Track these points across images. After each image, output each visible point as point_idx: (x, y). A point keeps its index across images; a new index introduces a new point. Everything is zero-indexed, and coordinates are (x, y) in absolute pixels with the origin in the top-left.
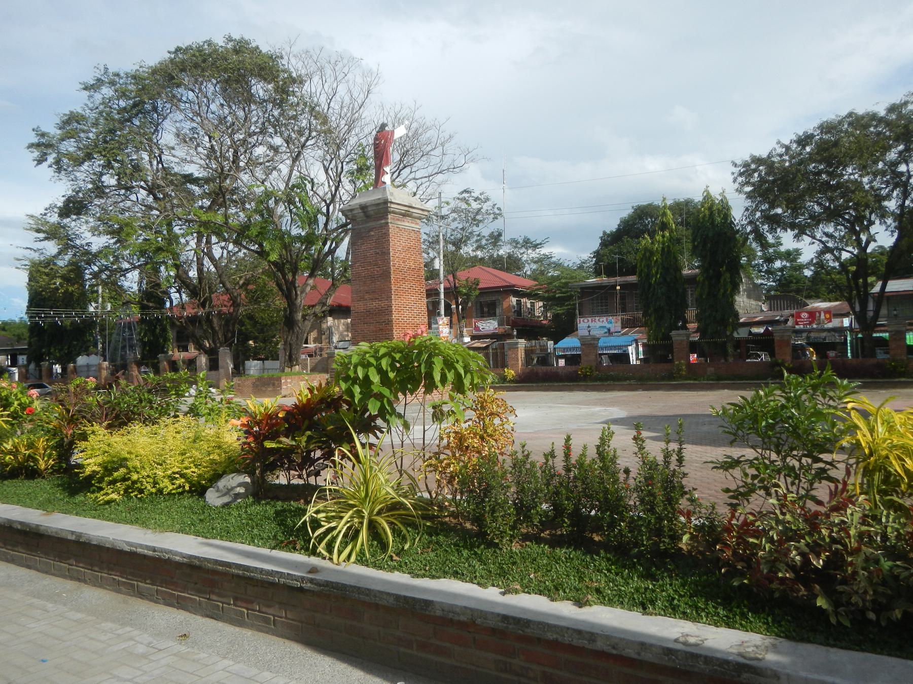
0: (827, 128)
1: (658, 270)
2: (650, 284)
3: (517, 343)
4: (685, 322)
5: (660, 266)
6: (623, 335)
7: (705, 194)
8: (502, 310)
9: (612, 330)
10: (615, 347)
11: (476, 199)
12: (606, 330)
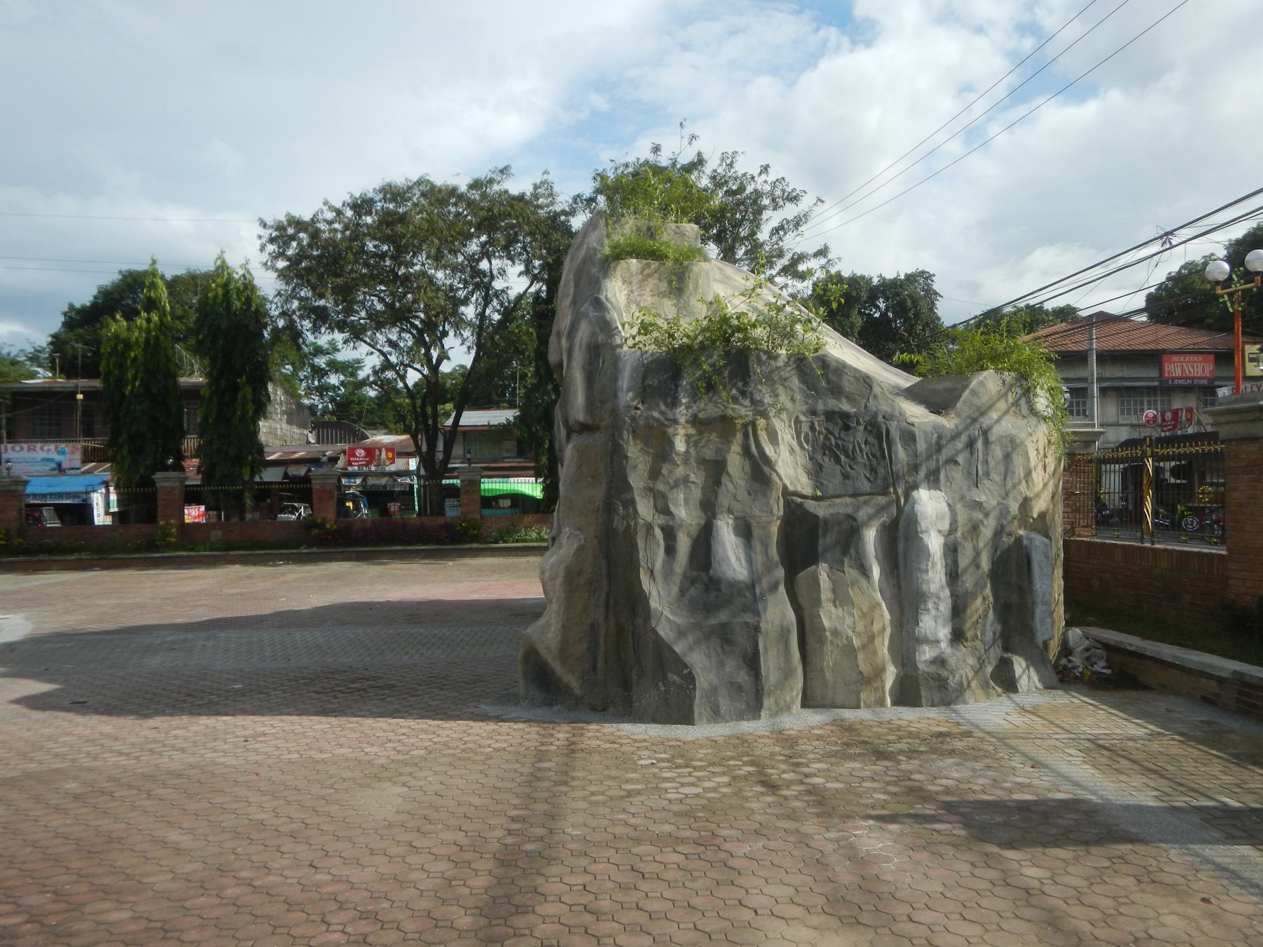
0: (392, 193)
1: (137, 371)
2: (124, 395)
4: (180, 457)
5: (141, 368)
6: (84, 473)
7: (219, 263)
9: (65, 465)
10: (68, 495)
12: (54, 466)
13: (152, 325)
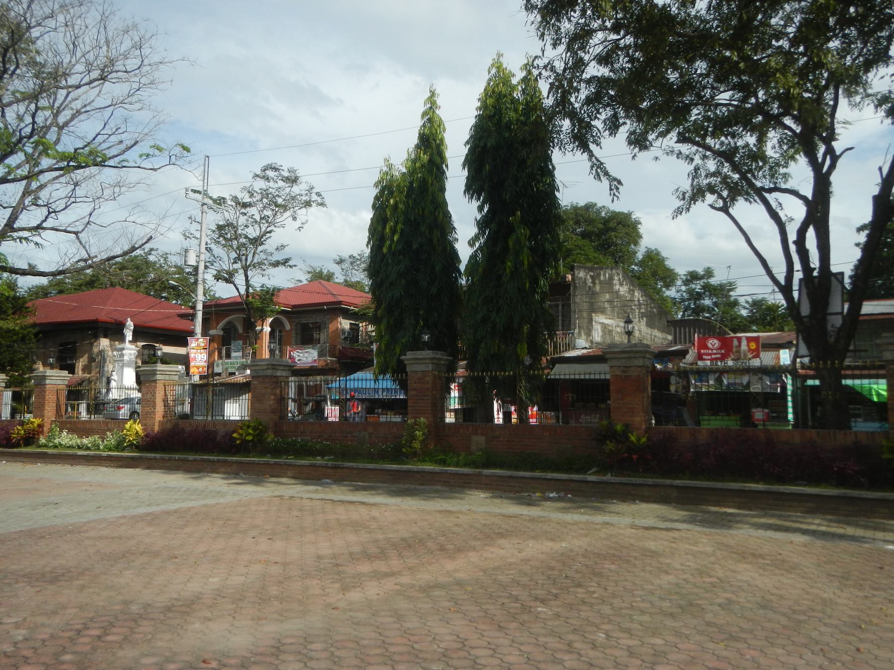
1: (395, 226)
3: (154, 373)
5: (401, 219)
7: (494, 71)
8: (328, 336)
11: (287, 180)
13: (418, 165)
